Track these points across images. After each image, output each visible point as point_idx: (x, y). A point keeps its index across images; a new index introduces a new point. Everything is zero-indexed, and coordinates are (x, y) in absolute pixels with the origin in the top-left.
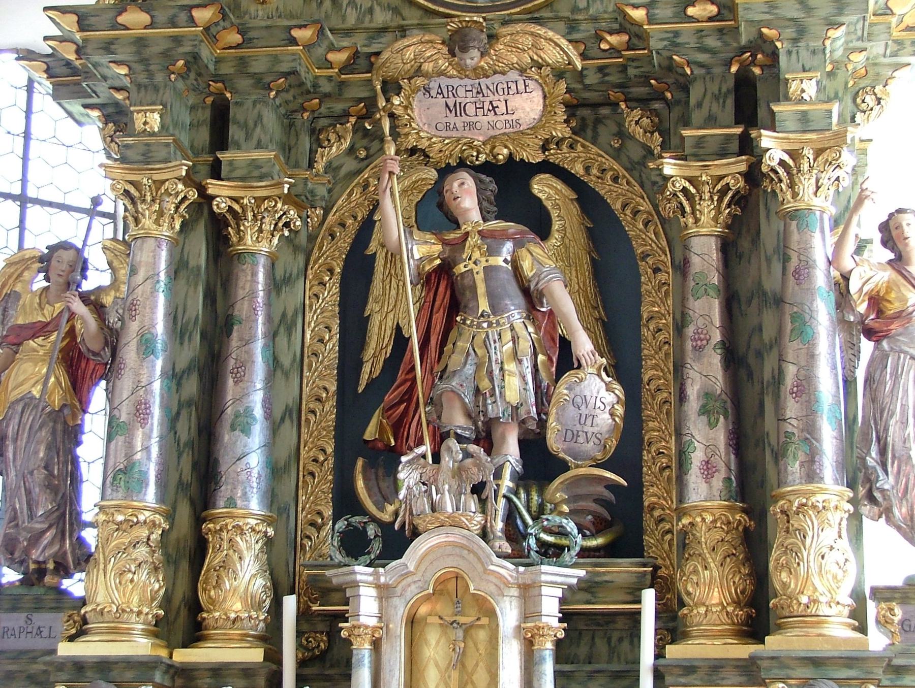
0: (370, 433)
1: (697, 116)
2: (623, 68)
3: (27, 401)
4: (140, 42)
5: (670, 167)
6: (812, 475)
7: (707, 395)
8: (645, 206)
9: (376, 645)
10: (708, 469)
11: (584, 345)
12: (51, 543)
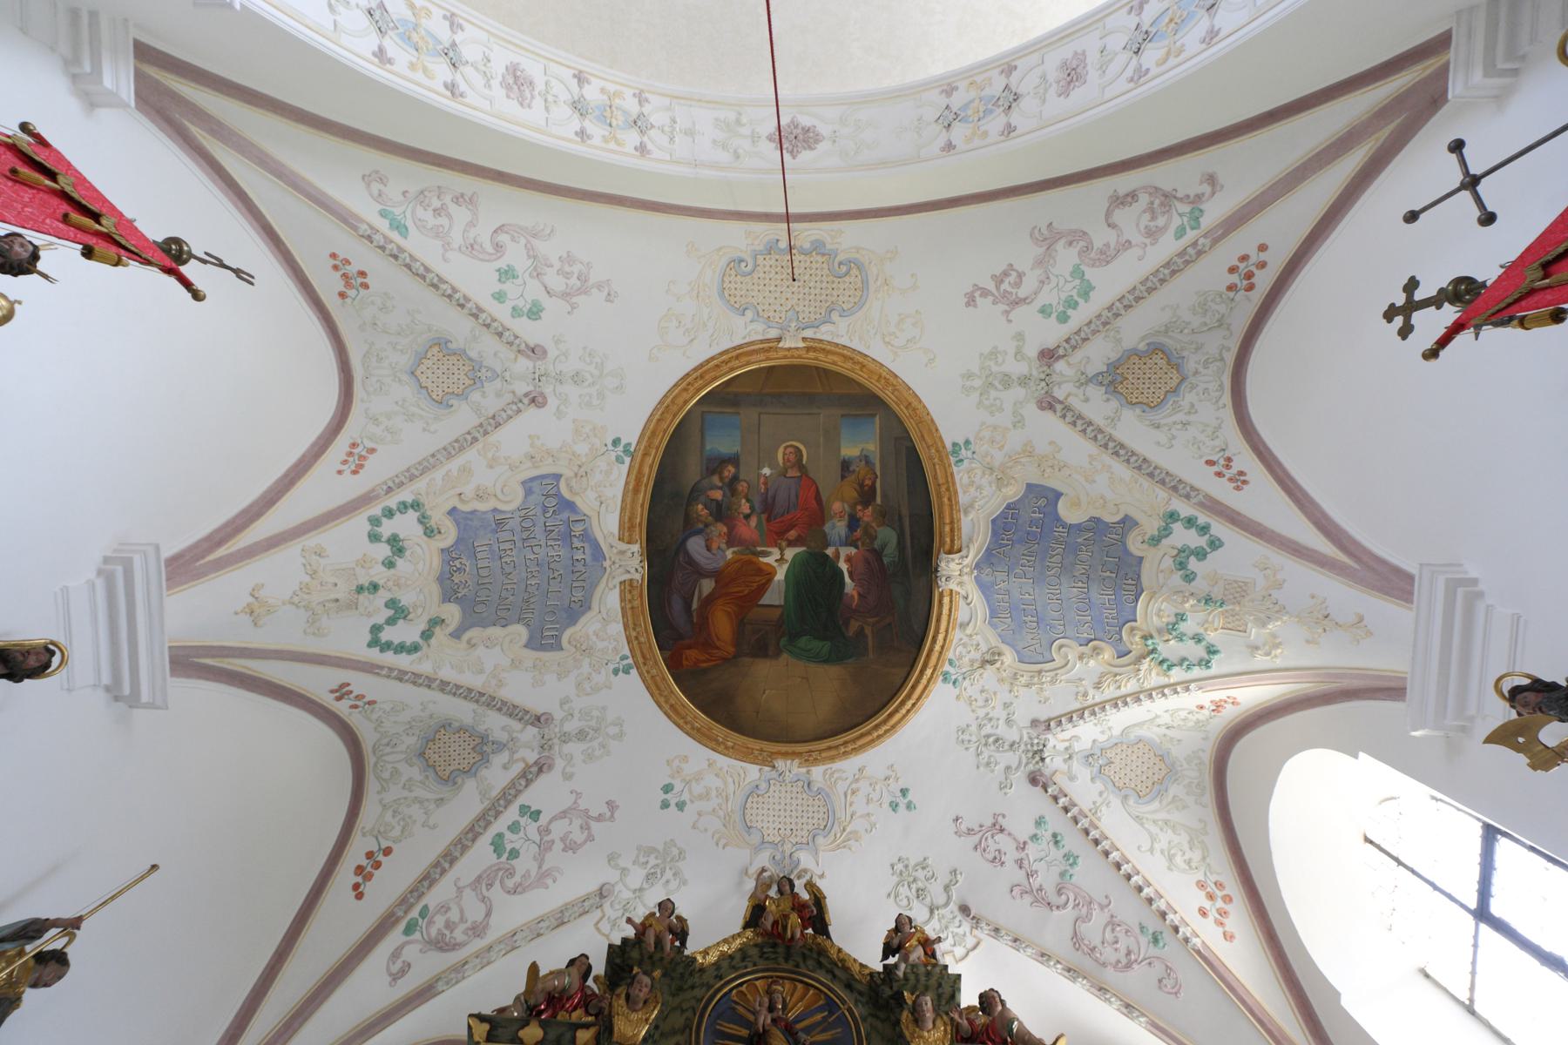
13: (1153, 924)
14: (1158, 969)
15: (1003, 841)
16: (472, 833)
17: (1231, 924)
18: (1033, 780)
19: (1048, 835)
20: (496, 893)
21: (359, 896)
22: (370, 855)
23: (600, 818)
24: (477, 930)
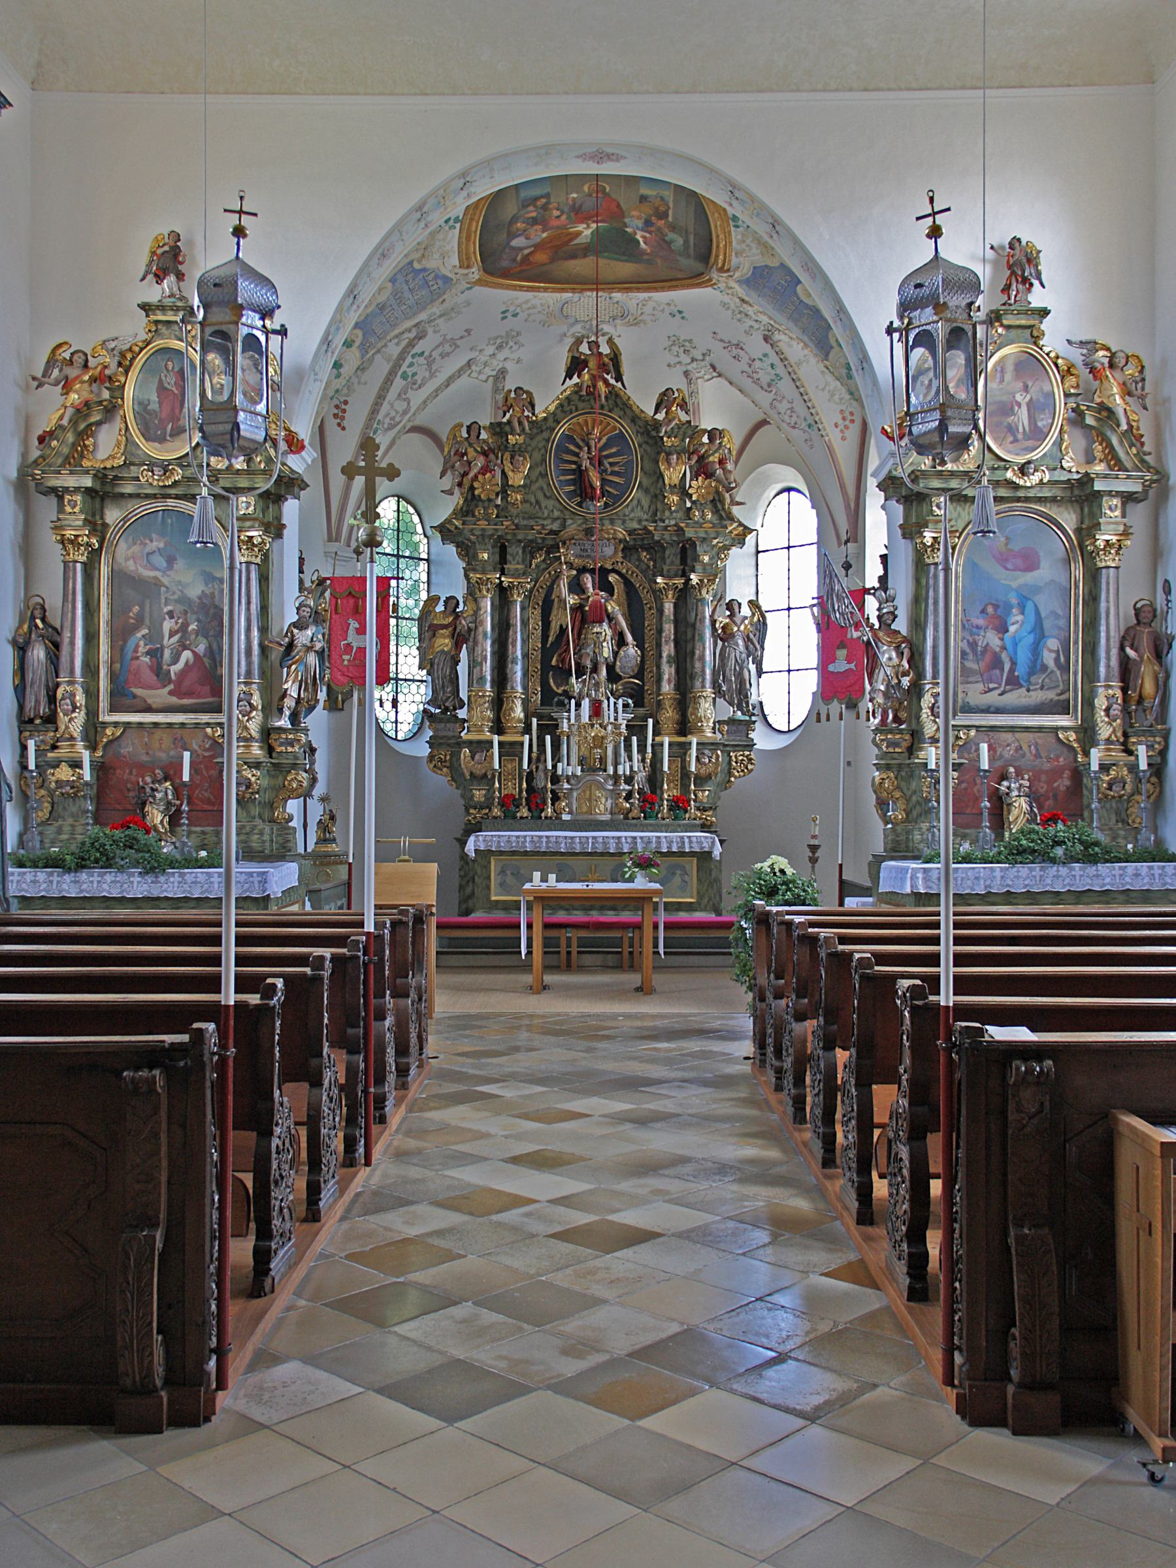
0: (554, 663)
1: (668, 561)
2: (643, 539)
3: (442, 651)
4: (483, 530)
5: (659, 580)
6: (703, 686)
7: (669, 656)
8: (647, 585)
9: (568, 737)
10: (669, 681)
11: (629, 638)
13: (810, 420)
14: (806, 436)
15: (742, 353)
17: (847, 433)
18: (766, 339)
19: (769, 362)
20: (410, 393)
21: (344, 429)
22: (337, 407)
23: (462, 337)
24: (405, 413)
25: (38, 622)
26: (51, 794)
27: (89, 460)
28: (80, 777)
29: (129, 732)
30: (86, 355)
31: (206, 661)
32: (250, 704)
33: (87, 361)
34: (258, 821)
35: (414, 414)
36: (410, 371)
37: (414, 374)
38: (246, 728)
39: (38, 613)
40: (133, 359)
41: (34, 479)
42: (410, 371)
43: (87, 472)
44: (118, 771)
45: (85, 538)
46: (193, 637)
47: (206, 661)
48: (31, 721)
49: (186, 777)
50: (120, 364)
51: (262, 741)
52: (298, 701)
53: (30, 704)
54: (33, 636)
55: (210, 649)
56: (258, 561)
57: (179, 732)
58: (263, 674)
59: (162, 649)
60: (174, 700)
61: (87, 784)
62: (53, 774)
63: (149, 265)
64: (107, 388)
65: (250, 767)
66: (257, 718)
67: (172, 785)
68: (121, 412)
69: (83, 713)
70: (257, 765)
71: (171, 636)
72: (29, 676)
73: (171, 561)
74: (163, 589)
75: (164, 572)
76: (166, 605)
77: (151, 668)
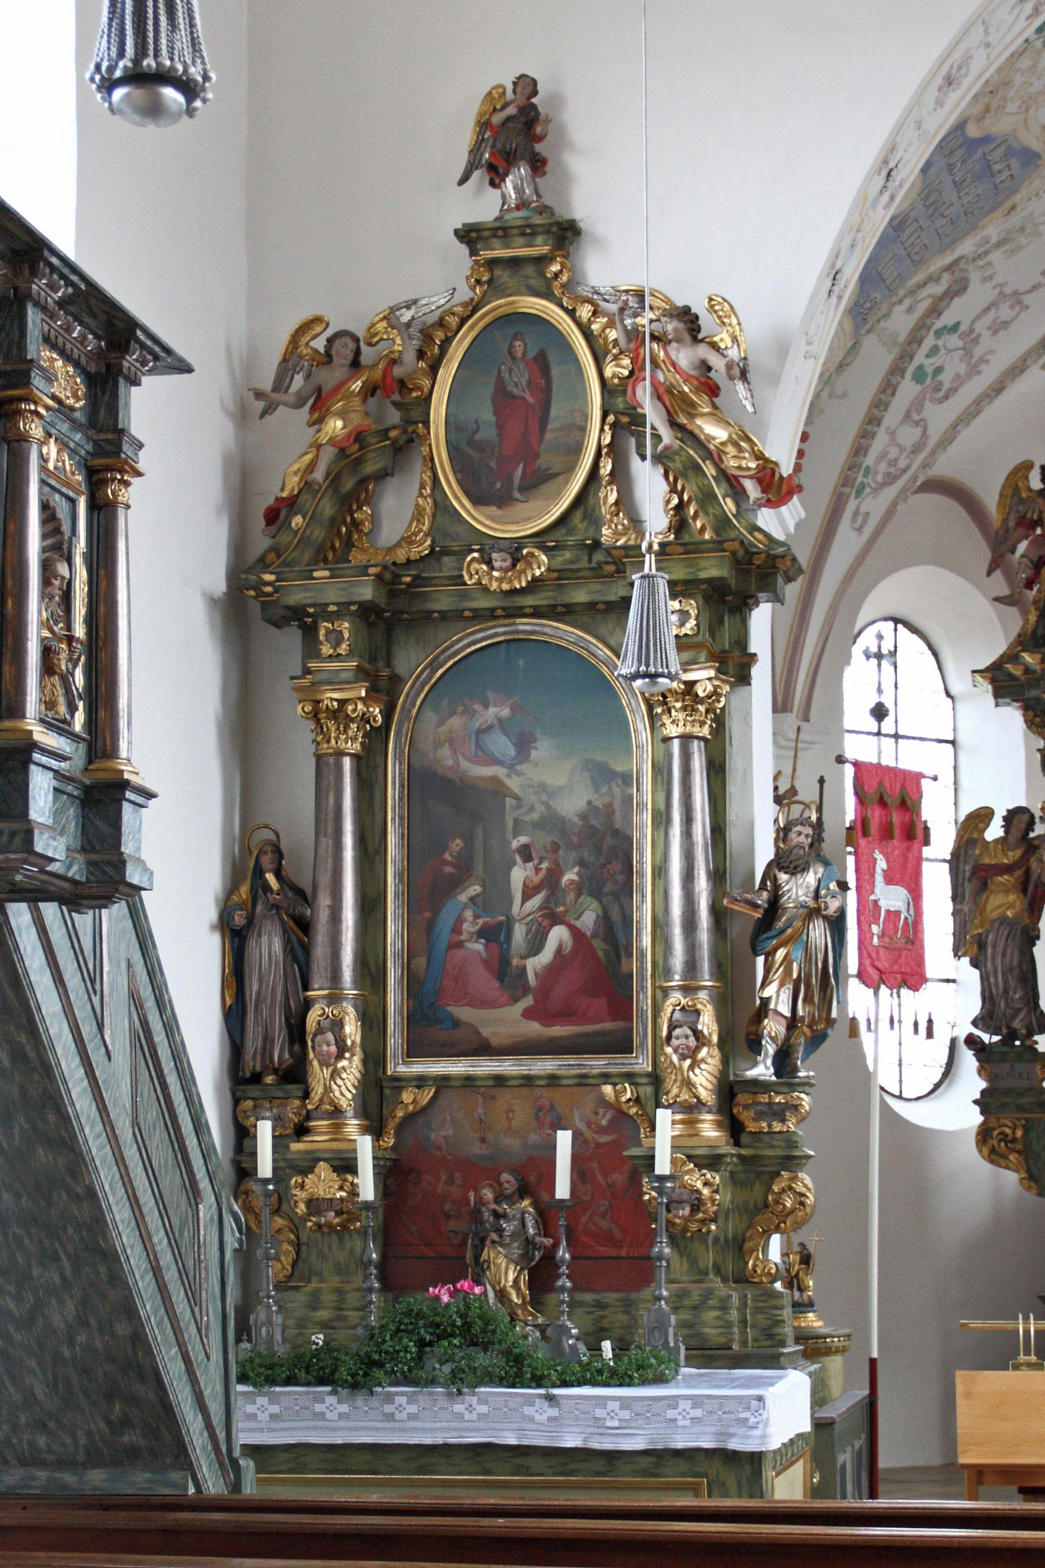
3: (1003, 920)
12: (1025, 1017)
16: (889, 387)
23: (1035, 288)
24: (916, 449)
25: (270, 877)
26: (295, 1225)
27: (364, 550)
28: (354, 1193)
29: (451, 1099)
30: (357, 340)
31: (599, 946)
32: (697, 1034)
33: (358, 352)
34: (716, 1283)
35: (933, 453)
36: (929, 365)
37: (939, 370)
38: (689, 1084)
39: (267, 861)
40: (447, 342)
41: (261, 594)
42: (929, 365)
43: (363, 571)
44: (427, 1178)
45: (360, 706)
46: (571, 897)
47: (599, 946)
48: (256, 1078)
49: (562, 1190)
50: (421, 354)
51: (719, 1111)
52: (793, 1023)
53: (252, 1045)
54: (259, 908)
55: (605, 920)
56: (705, 731)
57: (546, 1093)
58: (719, 970)
59: (508, 925)
60: (534, 1029)
61: (367, 1206)
62: (302, 1186)
63: (475, 151)
64: (397, 405)
65: (699, 1166)
66: (710, 1059)
67: (535, 1204)
68: (425, 450)
69: (357, 1060)
70: (711, 1161)
71: (527, 896)
72: (253, 987)
73: (524, 745)
74: (509, 802)
75: (511, 767)
76: (516, 834)
77: (487, 963)
